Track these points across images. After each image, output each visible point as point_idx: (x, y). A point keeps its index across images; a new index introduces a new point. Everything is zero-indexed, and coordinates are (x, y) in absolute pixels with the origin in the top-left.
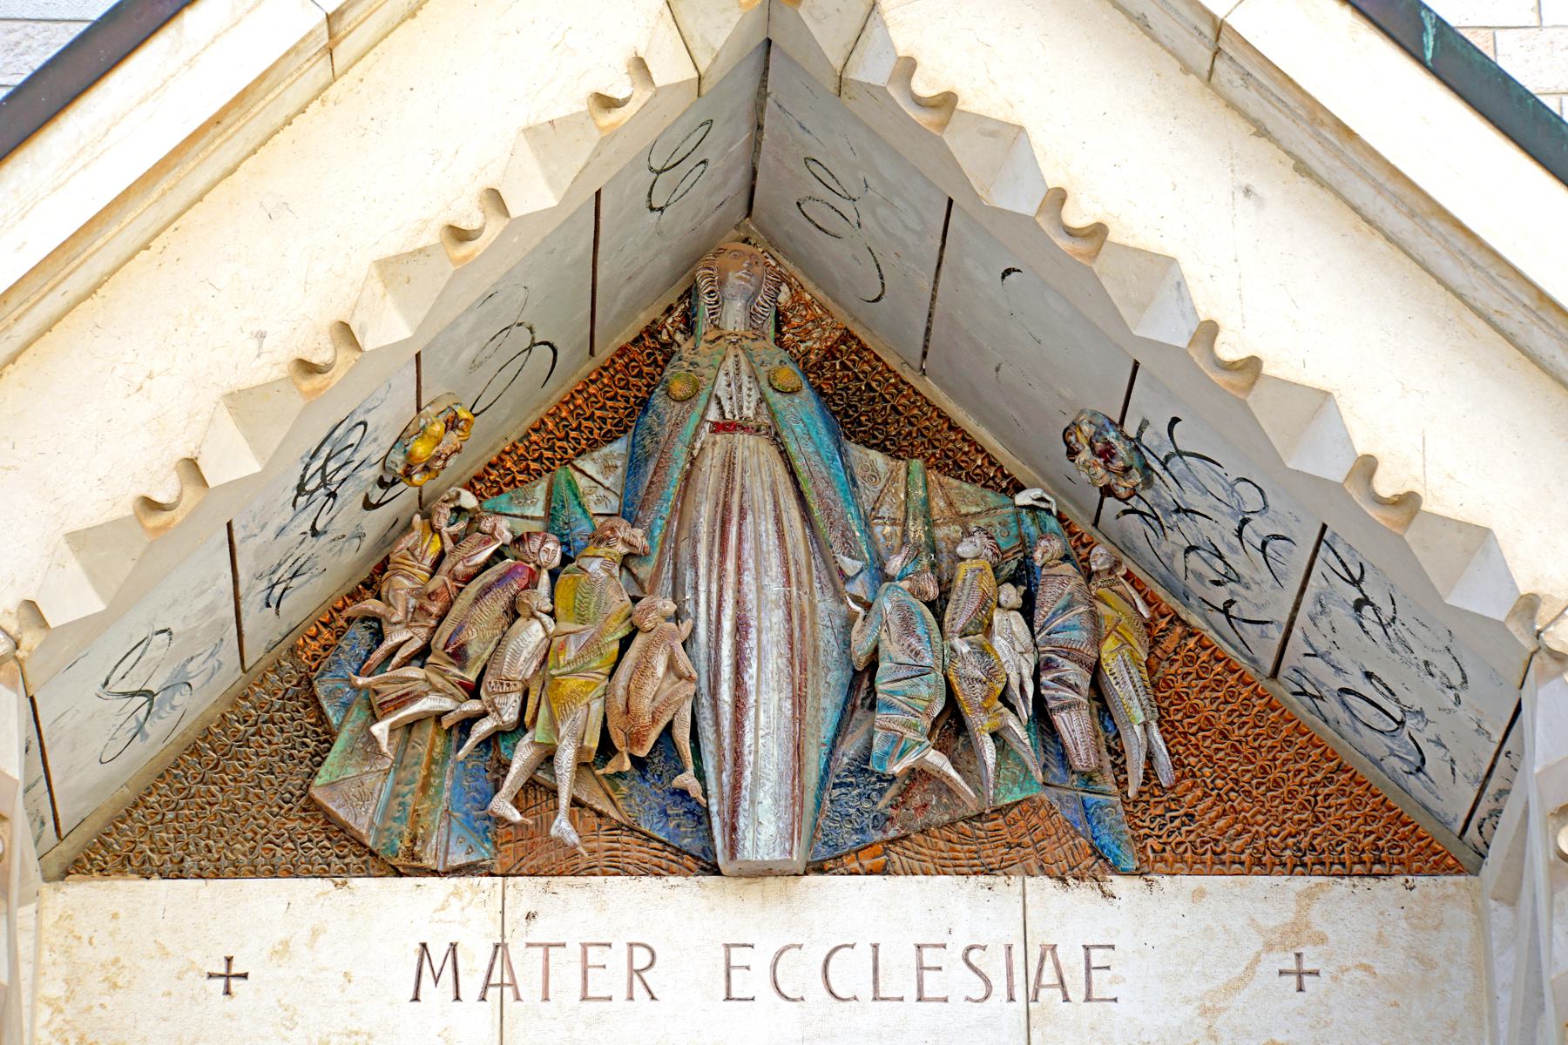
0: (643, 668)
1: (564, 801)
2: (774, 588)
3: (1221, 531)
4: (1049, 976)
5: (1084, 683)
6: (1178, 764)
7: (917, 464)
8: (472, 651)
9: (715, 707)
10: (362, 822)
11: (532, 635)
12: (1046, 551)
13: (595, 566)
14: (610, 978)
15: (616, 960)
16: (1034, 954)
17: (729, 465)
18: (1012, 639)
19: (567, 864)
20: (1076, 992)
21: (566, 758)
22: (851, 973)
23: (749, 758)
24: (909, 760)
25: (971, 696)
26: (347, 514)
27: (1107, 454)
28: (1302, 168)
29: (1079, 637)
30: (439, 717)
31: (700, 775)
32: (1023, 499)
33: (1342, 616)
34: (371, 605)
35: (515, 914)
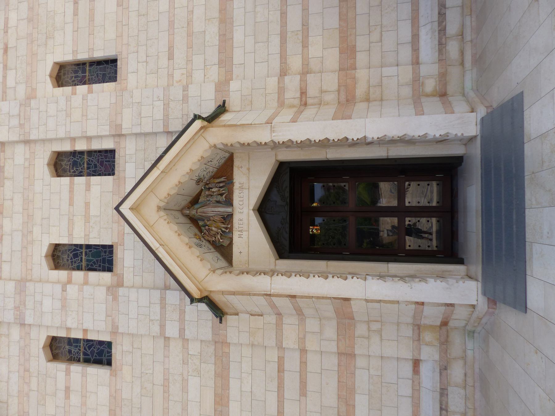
0: (216, 220)
1: (227, 226)
2: (210, 209)
3: (205, 173)
4: (241, 187)
5: (218, 184)
6: (225, 176)
7: (200, 197)
8: (215, 233)
9: (219, 214)
10: (228, 242)
11: (213, 229)
12: (207, 187)
13: (208, 223)
14: (241, 222)
15: (240, 222)
16: (240, 188)
17: (200, 212)
18: (214, 190)
19: (232, 226)
20: (243, 185)
21: (223, 226)
22: (241, 203)
23: (223, 211)
24: (224, 198)
25: (219, 193)
26: (203, 244)
27: (199, 181)
28: (174, 165)
29: (214, 184)
30: (220, 236)
31: (225, 215)
32: (203, 189)
33: (212, 163)
34: (211, 241)
35: (236, 230)
